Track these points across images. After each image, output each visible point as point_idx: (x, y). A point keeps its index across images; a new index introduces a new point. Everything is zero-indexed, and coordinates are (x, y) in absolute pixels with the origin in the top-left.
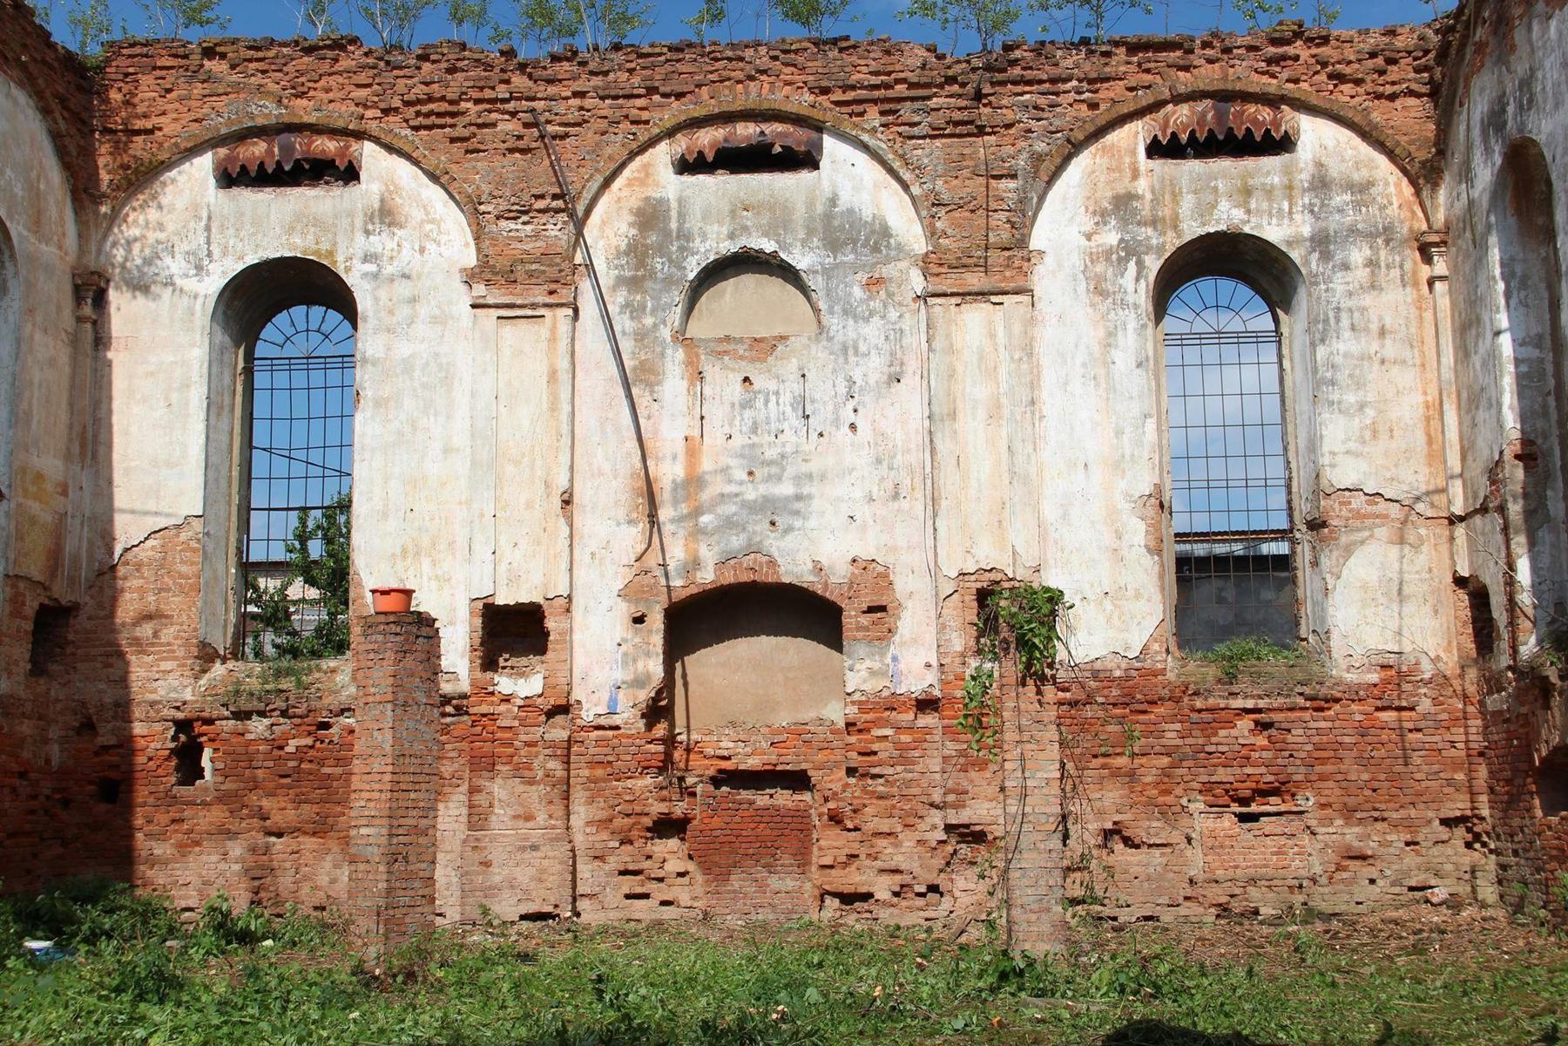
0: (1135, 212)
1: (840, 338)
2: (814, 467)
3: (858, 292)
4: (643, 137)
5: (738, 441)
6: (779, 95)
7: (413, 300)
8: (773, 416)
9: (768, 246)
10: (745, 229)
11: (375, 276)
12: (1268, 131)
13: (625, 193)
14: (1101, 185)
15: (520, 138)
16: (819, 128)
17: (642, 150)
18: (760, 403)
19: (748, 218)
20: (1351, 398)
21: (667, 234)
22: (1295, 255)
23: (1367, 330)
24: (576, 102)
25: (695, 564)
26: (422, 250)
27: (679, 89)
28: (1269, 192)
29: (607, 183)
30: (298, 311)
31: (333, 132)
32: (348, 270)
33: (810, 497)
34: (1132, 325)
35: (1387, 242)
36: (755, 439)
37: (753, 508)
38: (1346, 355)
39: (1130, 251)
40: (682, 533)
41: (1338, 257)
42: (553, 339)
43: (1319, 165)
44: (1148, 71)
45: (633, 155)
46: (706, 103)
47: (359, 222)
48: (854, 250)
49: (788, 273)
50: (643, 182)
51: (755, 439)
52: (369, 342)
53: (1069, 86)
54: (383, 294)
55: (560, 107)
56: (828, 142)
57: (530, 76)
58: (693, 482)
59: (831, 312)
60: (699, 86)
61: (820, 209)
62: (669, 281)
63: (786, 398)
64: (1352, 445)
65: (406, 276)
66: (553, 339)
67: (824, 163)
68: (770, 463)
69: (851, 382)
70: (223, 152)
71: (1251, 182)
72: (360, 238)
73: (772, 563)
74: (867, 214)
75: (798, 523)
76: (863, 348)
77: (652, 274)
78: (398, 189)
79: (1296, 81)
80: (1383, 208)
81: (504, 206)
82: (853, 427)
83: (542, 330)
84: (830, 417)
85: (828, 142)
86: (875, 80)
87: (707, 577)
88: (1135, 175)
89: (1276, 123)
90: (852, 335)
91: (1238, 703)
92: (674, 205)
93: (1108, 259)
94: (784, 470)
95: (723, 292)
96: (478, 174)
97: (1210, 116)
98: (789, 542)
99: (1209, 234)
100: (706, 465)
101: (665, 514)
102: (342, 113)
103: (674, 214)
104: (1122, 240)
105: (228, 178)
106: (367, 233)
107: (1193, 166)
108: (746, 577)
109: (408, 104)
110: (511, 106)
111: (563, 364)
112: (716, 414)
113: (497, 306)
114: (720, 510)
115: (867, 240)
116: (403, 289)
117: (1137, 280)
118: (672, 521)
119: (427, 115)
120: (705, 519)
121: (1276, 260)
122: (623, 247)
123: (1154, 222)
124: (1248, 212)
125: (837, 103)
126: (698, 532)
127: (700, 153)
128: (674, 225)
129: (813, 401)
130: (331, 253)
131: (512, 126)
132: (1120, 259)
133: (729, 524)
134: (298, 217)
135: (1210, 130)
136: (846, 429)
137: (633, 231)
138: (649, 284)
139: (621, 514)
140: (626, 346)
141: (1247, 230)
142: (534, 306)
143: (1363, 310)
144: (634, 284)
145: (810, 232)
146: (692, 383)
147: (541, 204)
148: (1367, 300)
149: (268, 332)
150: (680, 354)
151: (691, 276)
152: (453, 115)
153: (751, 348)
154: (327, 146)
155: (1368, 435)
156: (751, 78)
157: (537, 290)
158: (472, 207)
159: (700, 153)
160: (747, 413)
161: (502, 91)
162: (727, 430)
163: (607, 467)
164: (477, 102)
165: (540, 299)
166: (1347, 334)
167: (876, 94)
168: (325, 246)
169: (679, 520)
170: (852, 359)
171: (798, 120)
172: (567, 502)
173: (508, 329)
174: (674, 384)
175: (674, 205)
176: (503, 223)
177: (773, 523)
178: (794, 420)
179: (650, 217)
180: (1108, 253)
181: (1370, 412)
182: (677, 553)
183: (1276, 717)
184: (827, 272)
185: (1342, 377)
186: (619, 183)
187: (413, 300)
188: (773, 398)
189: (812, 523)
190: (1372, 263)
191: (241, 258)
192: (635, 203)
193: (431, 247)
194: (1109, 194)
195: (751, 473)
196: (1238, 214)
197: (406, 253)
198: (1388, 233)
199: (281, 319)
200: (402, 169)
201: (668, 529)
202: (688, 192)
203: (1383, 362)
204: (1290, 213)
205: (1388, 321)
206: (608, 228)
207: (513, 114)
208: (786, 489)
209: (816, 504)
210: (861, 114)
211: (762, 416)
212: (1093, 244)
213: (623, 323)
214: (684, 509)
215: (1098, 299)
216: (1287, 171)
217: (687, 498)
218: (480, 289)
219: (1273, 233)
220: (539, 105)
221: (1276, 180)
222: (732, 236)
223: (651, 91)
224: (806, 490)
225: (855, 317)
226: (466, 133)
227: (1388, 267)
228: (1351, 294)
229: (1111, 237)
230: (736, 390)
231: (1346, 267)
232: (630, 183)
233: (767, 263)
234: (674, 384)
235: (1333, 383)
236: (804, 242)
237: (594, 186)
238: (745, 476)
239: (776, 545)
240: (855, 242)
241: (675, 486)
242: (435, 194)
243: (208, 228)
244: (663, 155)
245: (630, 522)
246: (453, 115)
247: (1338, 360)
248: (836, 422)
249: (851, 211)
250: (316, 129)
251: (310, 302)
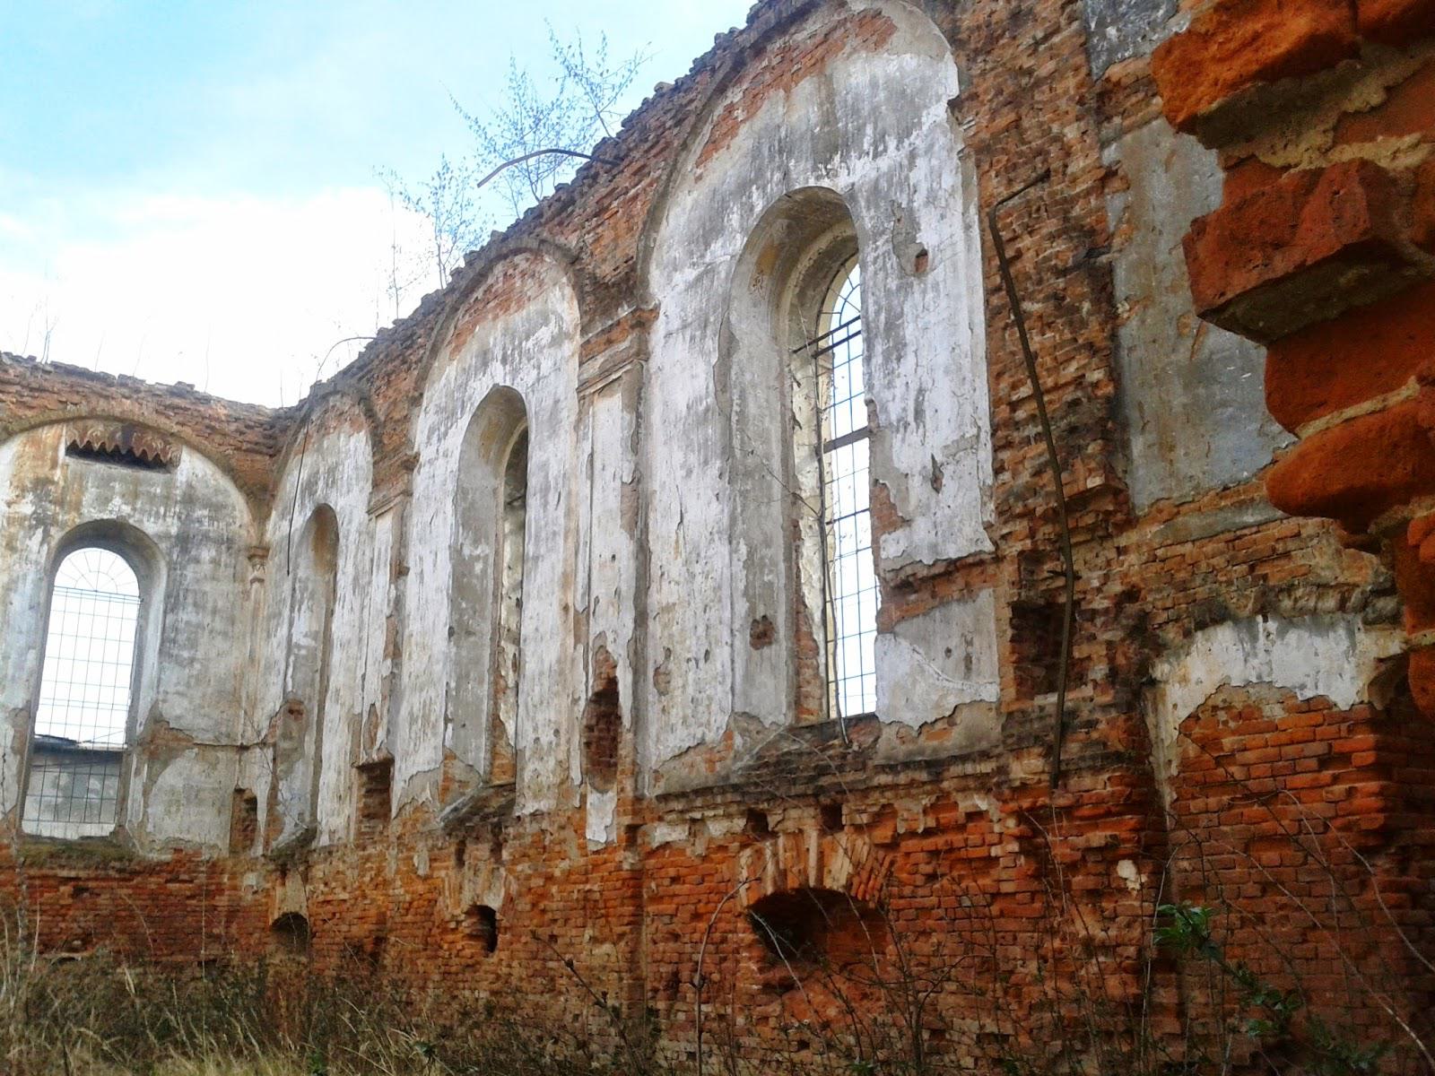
0: (48, 494)
12: (158, 455)
14: (26, 468)
20: (185, 654)
22: (163, 546)
23: (204, 608)
28: (152, 498)
34: (31, 577)
35: (229, 548)
38: (187, 623)
39: (42, 521)
41: (193, 553)
43: (190, 486)
44: (78, 393)
53: (14, 389)
64: (181, 688)
71: (140, 489)
79: (183, 425)
80: (228, 525)
88: (54, 465)
89: (165, 452)
91: (65, 873)
93: (21, 525)
97: (119, 435)
99: (102, 520)
104: (35, 512)
107: (100, 468)
117: (42, 544)
121: (148, 547)
123: (60, 503)
124: (134, 509)
132: (30, 527)
135: (117, 446)
141: (131, 521)
143: (205, 593)
148: (207, 587)
155: (193, 681)
166: (190, 609)
180: (25, 518)
181: (197, 666)
183: (91, 884)
185: (182, 638)
190: (215, 562)
194: (31, 476)
196: (126, 509)
198: (230, 542)
203: (211, 632)
204: (165, 515)
205: (220, 604)
212: (11, 510)
215: (9, 553)
216: (169, 485)
219: (151, 527)
221: (158, 491)
227: (226, 566)
228: (198, 581)
229: (26, 508)
231: (197, 561)
235: (174, 641)
247: (182, 626)
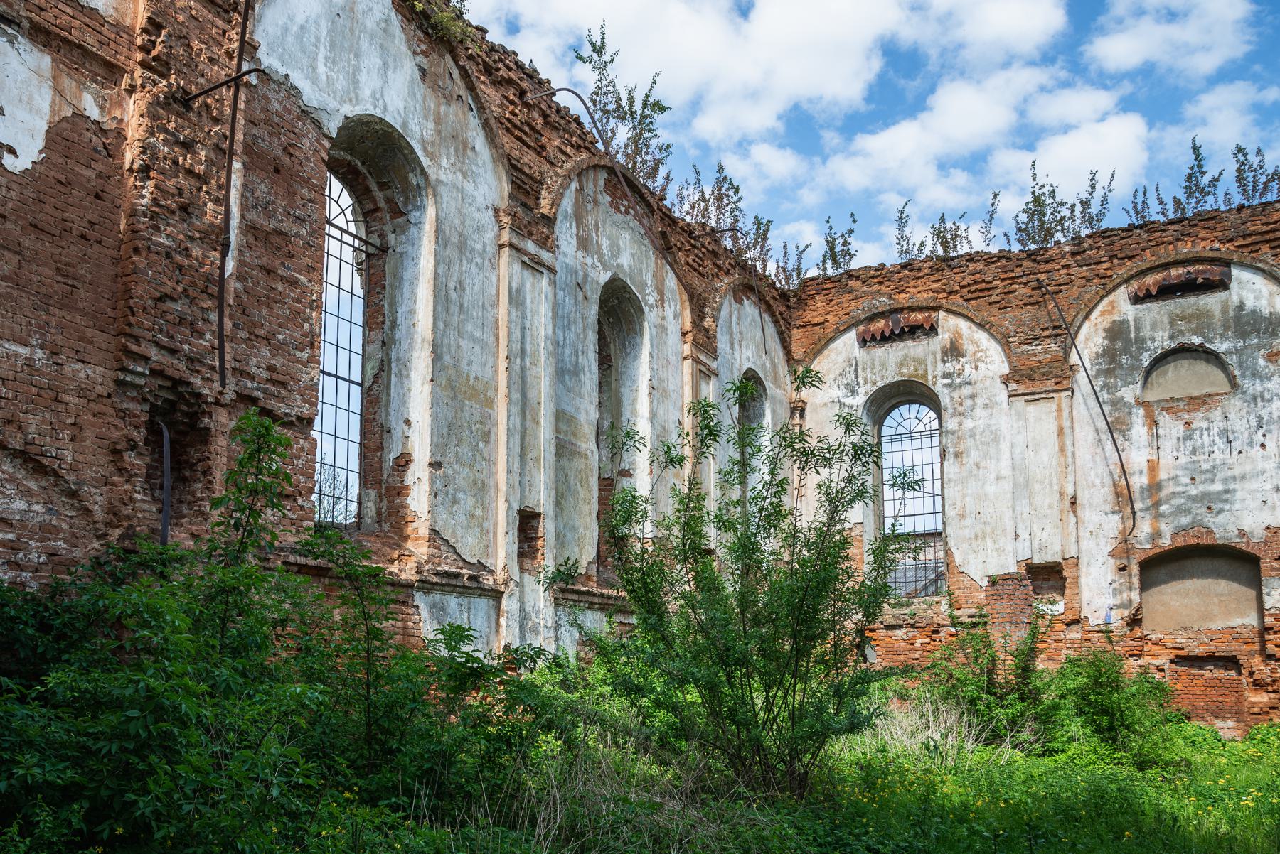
1: (1251, 391)
2: (1237, 471)
3: (1261, 362)
4: (1109, 287)
5: (1183, 460)
6: (1199, 248)
7: (973, 396)
8: (1206, 443)
9: (1197, 340)
10: (1181, 332)
11: (949, 385)
13: (1100, 319)
15: (1031, 296)
16: (1228, 264)
17: (1109, 293)
18: (1196, 436)
19: (1182, 325)
21: (1128, 342)
24: (1065, 271)
25: (1156, 535)
26: (977, 368)
27: (1129, 254)
29: (1087, 316)
30: (904, 409)
31: (920, 309)
32: (934, 384)
33: (1234, 491)
36: (1194, 458)
37: (1193, 499)
40: (1148, 517)
42: (1059, 410)
45: (1103, 297)
46: (1149, 259)
47: (939, 356)
48: (1258, 336)
49: (1213, 358)
50: (1110, 312)
51: (1194, 458)
52: (951, 424)
54: (956, 395)
55: (1056, 276)
56: (1235, 272)
57: (1034, 261)
58: (1154, 487)
59: (1243, 376)
60: (1144, 250)
61: (1231, 313)
62: (1132, 368)
63: (1215, 431)
65: (969, 383)
66: (1059, 410)
67: (1234, 285)
68: (1207, 471)
69: (1260, 418)
70: (861, 328)
72: (940, 366)
73: (1210, 532)
74: (1266, 312)
75: (1227, 507)
76: (1267, 396)
77: (1120, 366)
78: (960, 335)
81: (1023, 337)
82: (1263, 446)
83: (1053, 406)
84: (1246, 441)
85: (1235, 272)
86: (1265, 228)
87: (1166, 542)
90: (1259, 388)
92: (1132, 323)
94: (1215, 475)
95: (1166, 373)
96: (1006, 321)
98: (1221, 519)
100: (1163, 475)
101: (1138, 506)
102: (924, 297)
103: (1132, 328)
105: (863, 342)
106: (944, 362)
108: (1192, 542)
109: (962, 287)
110: (1024, 279)
111: (1066, 424)
112: (1168, 446)
113: (1024, 395)
114: (1173, 502)
115: (1267, 328)
116: (967, 390)
118: (1141, 510)
119: (976, 290)
120: (1163, 508)
122: (1100, 350)
125: (1239, 247)
126: (1158, 516)
127: (1148, 290)
128: (1133, 335)
129: (1233, 432)
130: (925, 375)
131: (1026, 291)
133: (1179, 511)
134: (905, 357)
136: (1258, 447)
137: (1106, 342)
138: (1118, 372)
139: (1108, 508)
140: (1107, 409)
142: (1047, 392)
144: (1108, 373)
145: (1226, 328)
146: (1150, 428)
147: (1047, 333)
149: (888, 421)
150: (1141, 411)
151: (1146, 364)
152: (989, 289)
153: (1189, 404)
154: (918, 317)
156: (1178, 240)
157: (1048, 383)
158: (1003, 340)
159: (1148, 290)
160: (1189, 443)
161: (1018, 271)
162: (1175, 454)
163: (1098, 482)
164: (1003, 280)
165: (1051, 388)
167: (1267, 237)
168: (921, 372)
169: (1147, 509)
170: (1260, 404)
171: (1212, 261)
172: (1073, 503)
173: (1032, 408)
174: (1139, 430)
175: (1132, 323)
176: (1023, 347)
177: (1209, 508)
178: (1221, 443)
179: (1116, 332)
182: (1144, 528)
184: (1238, 352)
186: (1095, 314)
187: (973, 396)
188: (1206, 433)
189: (1237, 506)
191: (874, 384)
192: (1106, 324)
193: (982, 365)
195: (1193, 479)
197: (967, 371)
199: (895, 413)
200: (963, 325)
201: (1139, 515)
202: (1141, 315)
206: (1090, 341)
207: (1026, 284)
208: (1218, 487)
209: (1239, 495)
210: (1257, 251)
211: (1199, 444)
213: (1105, 396)
214: (1149, 503)
217: (1150, 497)
218: (1013, 386)
220: (1042, 277)
222: (1171, 337)
223: (1111, 257)
224: (1231, 486)
225: (1261, 378)
226: (998, 299)
230: (1180, 429)
232: (1102, 314)
233: (1196, 351)
234: (1139, 430)
236: (1222, 336)
237: (1080, 317)
238: (1188, 481)
239: (1209, 520)
240: (1258, 331)
241: (1142, 490)
242: (982, 336)
243: (856, 370)
244: (1122, 294)
245: (1113, 512)
246: (989, 289)
248: (1251, 444)
249: (1254, 312)
250: (911, 309)
251: (910, 402)
